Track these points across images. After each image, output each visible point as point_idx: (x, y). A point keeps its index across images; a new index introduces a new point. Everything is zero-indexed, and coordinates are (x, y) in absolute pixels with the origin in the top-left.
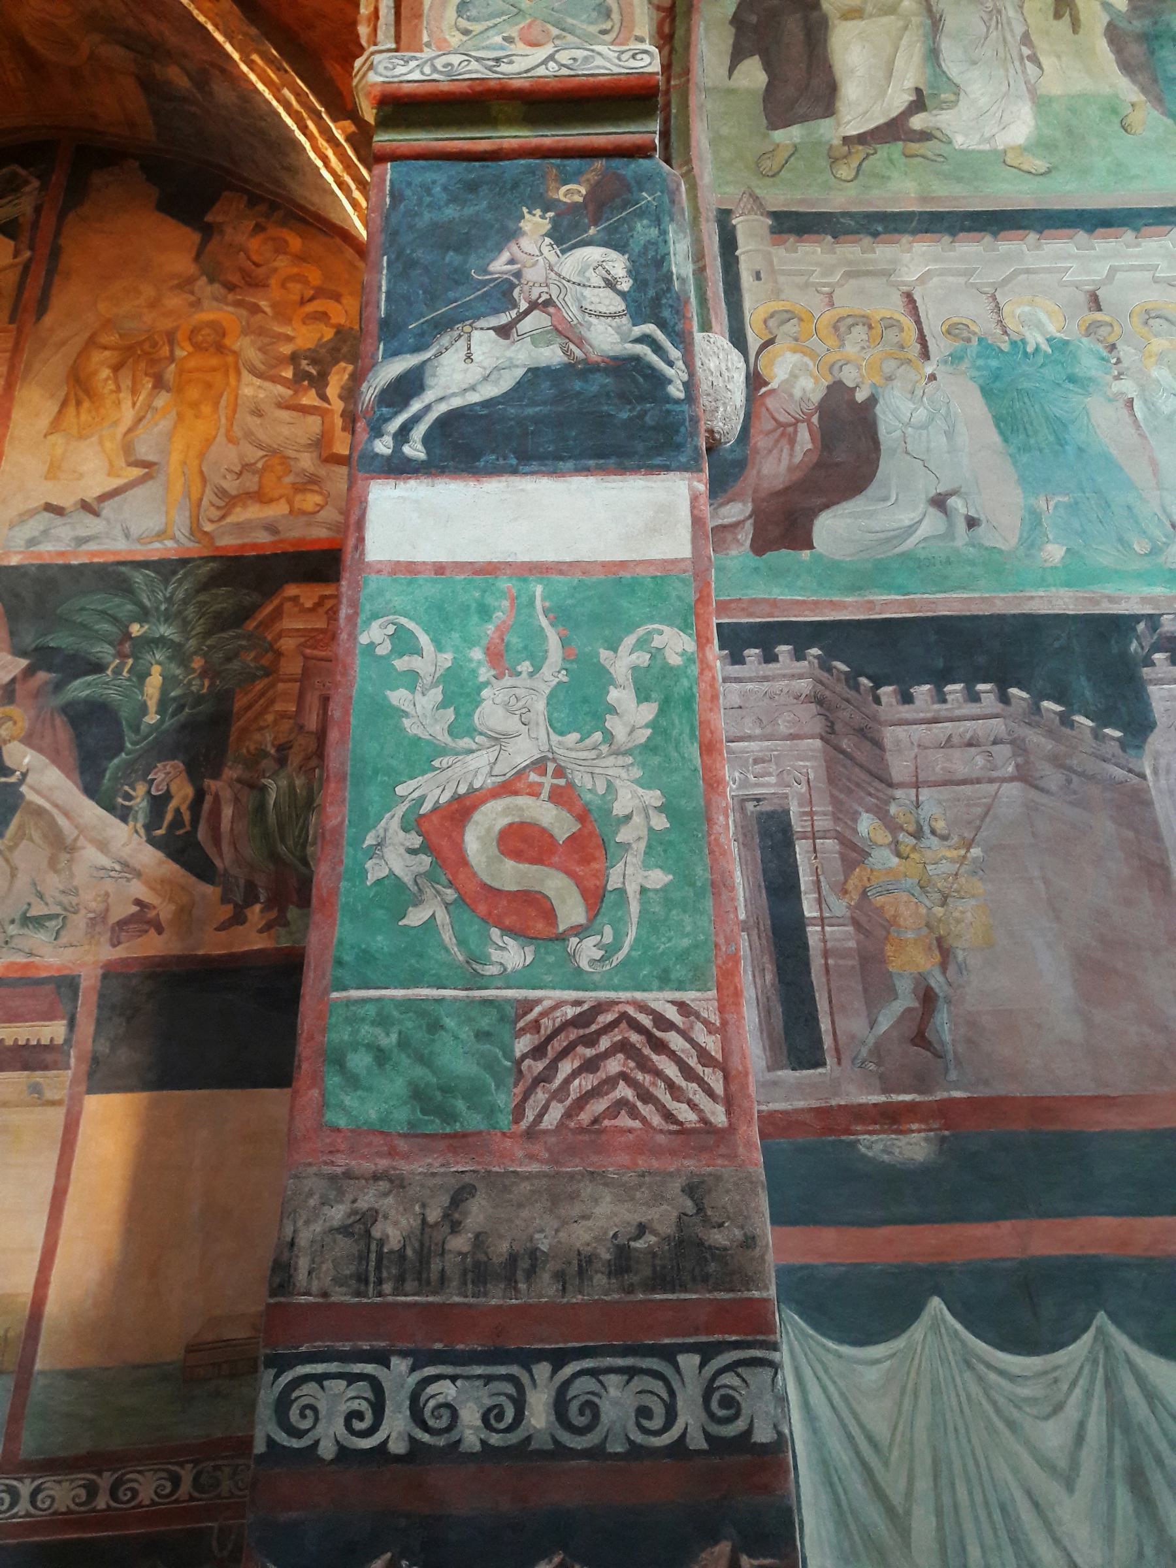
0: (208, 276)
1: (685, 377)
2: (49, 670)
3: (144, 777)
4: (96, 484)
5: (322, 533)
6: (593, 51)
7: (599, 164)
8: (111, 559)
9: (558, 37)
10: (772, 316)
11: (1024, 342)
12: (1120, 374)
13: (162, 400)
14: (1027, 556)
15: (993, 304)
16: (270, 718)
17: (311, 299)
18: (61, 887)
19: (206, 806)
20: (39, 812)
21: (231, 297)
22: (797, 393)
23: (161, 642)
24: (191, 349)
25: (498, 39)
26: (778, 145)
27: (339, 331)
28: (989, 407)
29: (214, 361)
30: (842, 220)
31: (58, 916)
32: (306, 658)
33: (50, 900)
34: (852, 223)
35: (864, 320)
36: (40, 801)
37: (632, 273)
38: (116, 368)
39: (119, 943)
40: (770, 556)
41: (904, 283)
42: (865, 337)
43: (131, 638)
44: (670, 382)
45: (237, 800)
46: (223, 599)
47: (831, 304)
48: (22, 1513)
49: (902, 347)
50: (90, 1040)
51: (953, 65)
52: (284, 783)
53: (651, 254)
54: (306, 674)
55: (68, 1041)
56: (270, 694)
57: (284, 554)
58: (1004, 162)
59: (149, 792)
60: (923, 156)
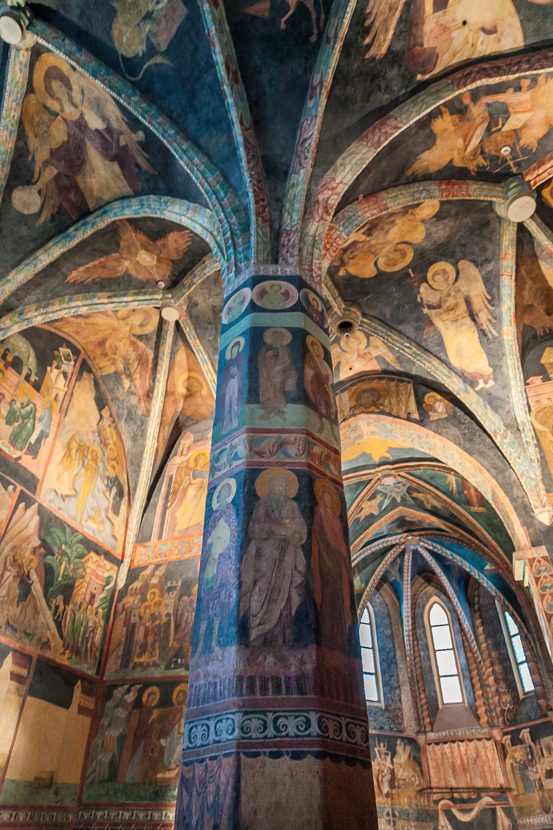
4: (66, 492)
5: (101, 540)
16: (80, 593)
20: (34, 597)
23: (66, 554)
29: (94, 466)
32: (90, 578)
38: (77, 451)
46: (81, 549)
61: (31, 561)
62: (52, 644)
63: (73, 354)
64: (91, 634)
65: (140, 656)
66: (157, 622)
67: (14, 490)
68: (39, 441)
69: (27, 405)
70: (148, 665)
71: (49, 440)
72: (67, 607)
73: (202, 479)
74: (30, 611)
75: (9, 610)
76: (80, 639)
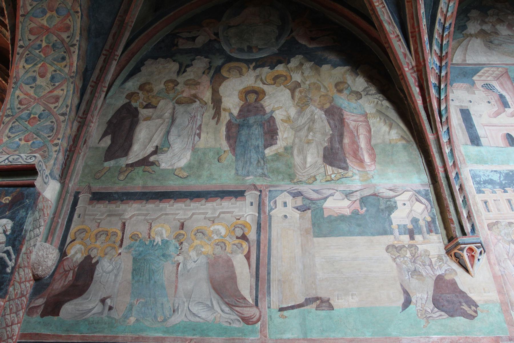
1: (13, 265)
6: (20, 156)
7: (18, 189)
9: (35, 138)
10: (78, 231)
11: (154, 241)
12: (180, 253)
14: (123, 321)
15: (149, 227)
22: (75, 259)
25: (17, 139)
26: (104, 168)
28: (133, 265)
30: (114, 195)
34: (117, 196)
35: (106, 232)
37: (13, 229)
40: (44, 318)
41: (124, 219)
42: (104, 239)
44: (8, 266)
47: (98, 227)
49: (115, 243)
51: (171, 138)
53: (21, 221)
58: (174, 174)
60: (148, 172)
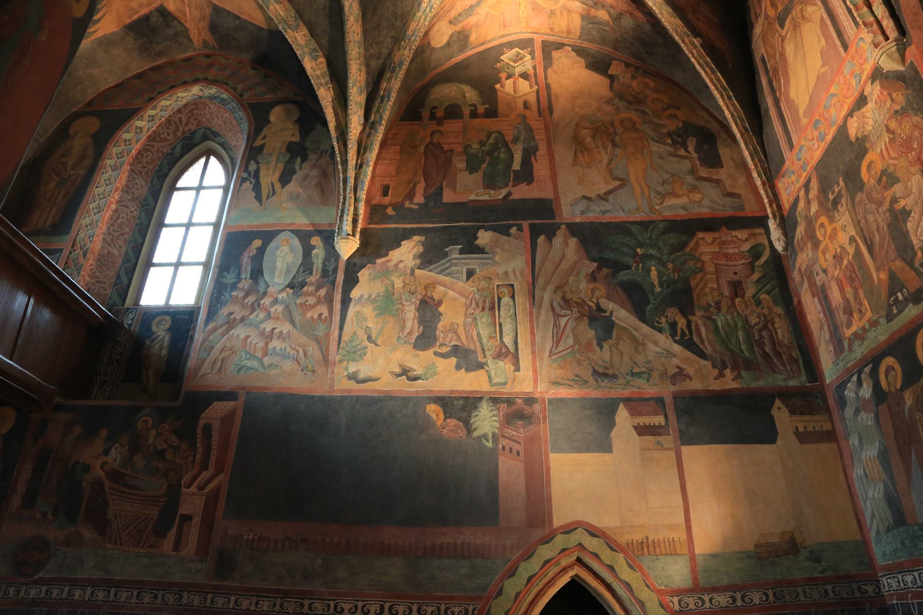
0: (618, 97)
2: (607, 268)
3: (663, 315)
4: (603, 189)
5: (707, 210)
8: (619, 220)
13: (618, 151)
16: (708, 290)
17: (667, 109)
18: (643, 360)
19: (693, 327)
20: (624, 328)
21: (631, 107)
23: (651, 256)
24: (623, 130)
27: (684, 123)
29: (635, 135)
31: (645, 372)
32: (715, 264)
33: (640, 366)
36: (623, 324)
38: (593, 137)
39: (675, 384)
43: (639, 255)
45: (705, 325)
46: (673, 239)
48: (708, 607)
50: (676, 424)
52: (723, 318)
54: (717, 272)
55: (667, 424)
56: (704, 279)
57: (693, 219)
59: (667, 321)
61: (593, 291)
62: (691, 371)
63: (522, 49)
64: (764, 333)
65: (849, 325)
66: (845, 262)
67: (520, 228)
68: (527, 163)
69: (488, 139)
70: (864, 330)
71: (542, 151)
72: (690, 317)
73: (790, 16)
74: (625, 346)
75: (589, 359)
76: (743, 347)
